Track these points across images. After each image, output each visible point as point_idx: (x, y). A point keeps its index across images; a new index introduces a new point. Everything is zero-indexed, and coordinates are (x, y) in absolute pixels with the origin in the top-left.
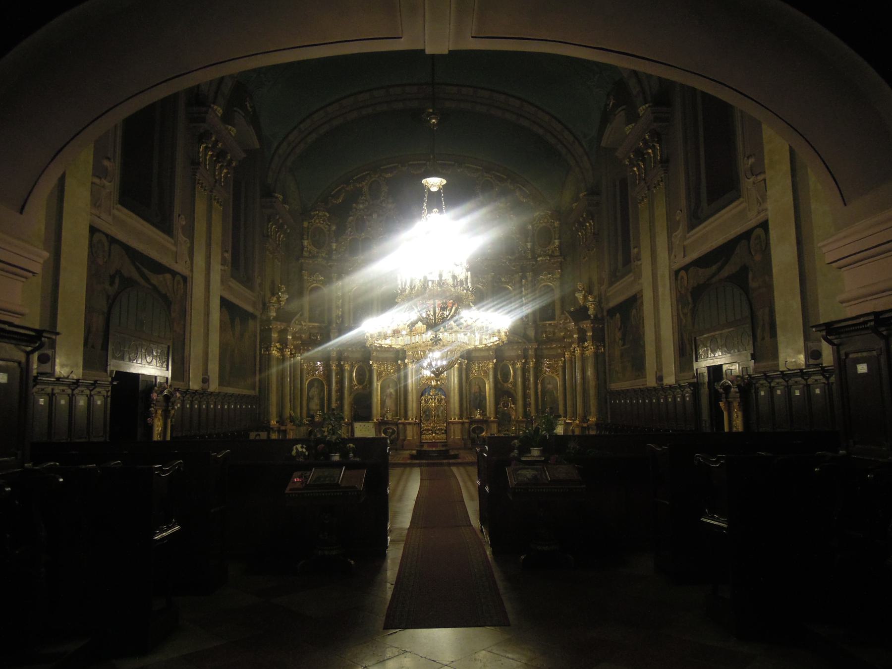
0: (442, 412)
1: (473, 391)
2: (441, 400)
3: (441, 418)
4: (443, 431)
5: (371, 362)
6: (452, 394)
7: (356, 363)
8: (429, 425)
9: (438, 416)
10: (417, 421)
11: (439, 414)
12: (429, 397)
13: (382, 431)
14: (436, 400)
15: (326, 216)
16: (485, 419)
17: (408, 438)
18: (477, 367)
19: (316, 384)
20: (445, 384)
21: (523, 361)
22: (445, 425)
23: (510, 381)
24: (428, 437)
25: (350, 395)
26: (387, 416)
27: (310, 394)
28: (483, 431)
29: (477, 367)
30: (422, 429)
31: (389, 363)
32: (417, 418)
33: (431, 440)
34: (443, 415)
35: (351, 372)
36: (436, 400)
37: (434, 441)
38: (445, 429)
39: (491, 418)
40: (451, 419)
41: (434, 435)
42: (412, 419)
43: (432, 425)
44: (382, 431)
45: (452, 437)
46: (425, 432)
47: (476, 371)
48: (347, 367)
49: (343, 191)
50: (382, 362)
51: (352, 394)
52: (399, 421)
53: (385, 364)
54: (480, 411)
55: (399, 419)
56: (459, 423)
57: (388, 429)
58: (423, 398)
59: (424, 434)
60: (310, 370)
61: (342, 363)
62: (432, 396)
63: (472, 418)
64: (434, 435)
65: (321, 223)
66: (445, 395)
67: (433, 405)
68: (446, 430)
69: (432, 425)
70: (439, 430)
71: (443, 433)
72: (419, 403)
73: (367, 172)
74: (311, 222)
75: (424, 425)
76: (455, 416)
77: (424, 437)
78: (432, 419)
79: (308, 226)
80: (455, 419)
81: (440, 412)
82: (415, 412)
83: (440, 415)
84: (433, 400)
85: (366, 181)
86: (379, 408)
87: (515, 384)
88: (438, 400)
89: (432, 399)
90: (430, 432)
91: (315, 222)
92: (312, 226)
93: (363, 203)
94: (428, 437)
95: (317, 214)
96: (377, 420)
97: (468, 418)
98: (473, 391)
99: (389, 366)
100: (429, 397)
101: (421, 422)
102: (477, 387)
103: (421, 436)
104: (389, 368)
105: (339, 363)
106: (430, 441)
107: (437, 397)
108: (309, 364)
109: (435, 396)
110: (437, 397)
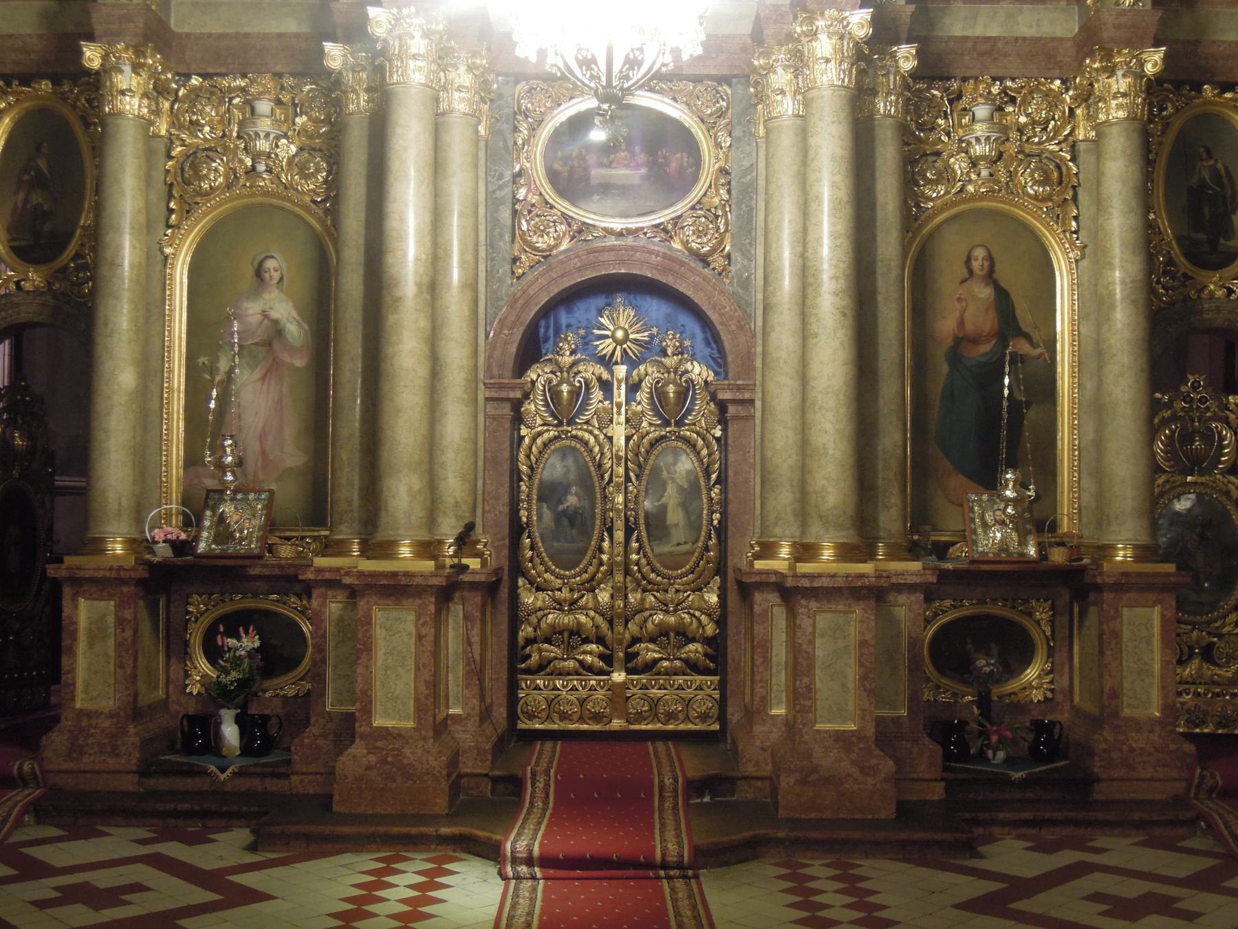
0: (691, 492)
1: (945, 326)
2: (682, 394)
3: (679, 534)
4: (694, 649)
5: (92, 56)
6: (783, 339)
8: (587, 599)
9: (657, 525)
10: (474, 563)
11: (663, 510)
12: (590, 370)
13: (195, 638)
14: (643, 395)
16: (1058, 556)
17: (379, 722)
18: (980, 129)
20: (718, 262)
22: (714, 599)
24: (568, 690)
26: (222, 519)
28: (1026, 662)
29: (980, 129)
30: (526, 631)
31: (267, 82)
32: (483, 538)
33: (597, 717)
34: (694, 526)
36: (643, 395)
37: (617, 724)
38: (710, 629)
39: (1105, 550)
40: (768, 550)
41: (619, 677)
42: (428, 548)
43: (604, 596)
44: (195, 638)
45: (779, 711)
46: (552, 651)
47: (974, 163)
50: (204, 76)
52: (320, 562)
54: (1022, 485)
55: (330, 547)
56: (856, 591)
57: (234, 623)
58: (538, 375)
59: (541, 668)
62: (607, 362)
63: (941, 550)
64: (619, 677)
66: (719, 361)
67: (619, 432)
68: (717, 646)
69: (604, 596)
70: (660, 635)
71: (692, 666)
72: (506, 410)
75: (542, 599)
76: (815, 532)
77: (535, 691)
78: (610, 550)
80: (805, 551)
81: (671, 496)
82: (454, 485)
83: (675, 516)
84: (620, 394)
86: (176, 452)
88: (658, 394)
89: (606, 386)
90: (590, 653)
94: (568, 690)
96: (139, 545)
97: (913, 551)
98: (945, 326)
99: (264, 107)
100: (590, 370)
101: (517, 569)
102: (985, 292)
103: (513, 686)
104: (265, 125)
106: (597, 727)
107: (650, 373)
109: (633, 364)
110: (650, 373)
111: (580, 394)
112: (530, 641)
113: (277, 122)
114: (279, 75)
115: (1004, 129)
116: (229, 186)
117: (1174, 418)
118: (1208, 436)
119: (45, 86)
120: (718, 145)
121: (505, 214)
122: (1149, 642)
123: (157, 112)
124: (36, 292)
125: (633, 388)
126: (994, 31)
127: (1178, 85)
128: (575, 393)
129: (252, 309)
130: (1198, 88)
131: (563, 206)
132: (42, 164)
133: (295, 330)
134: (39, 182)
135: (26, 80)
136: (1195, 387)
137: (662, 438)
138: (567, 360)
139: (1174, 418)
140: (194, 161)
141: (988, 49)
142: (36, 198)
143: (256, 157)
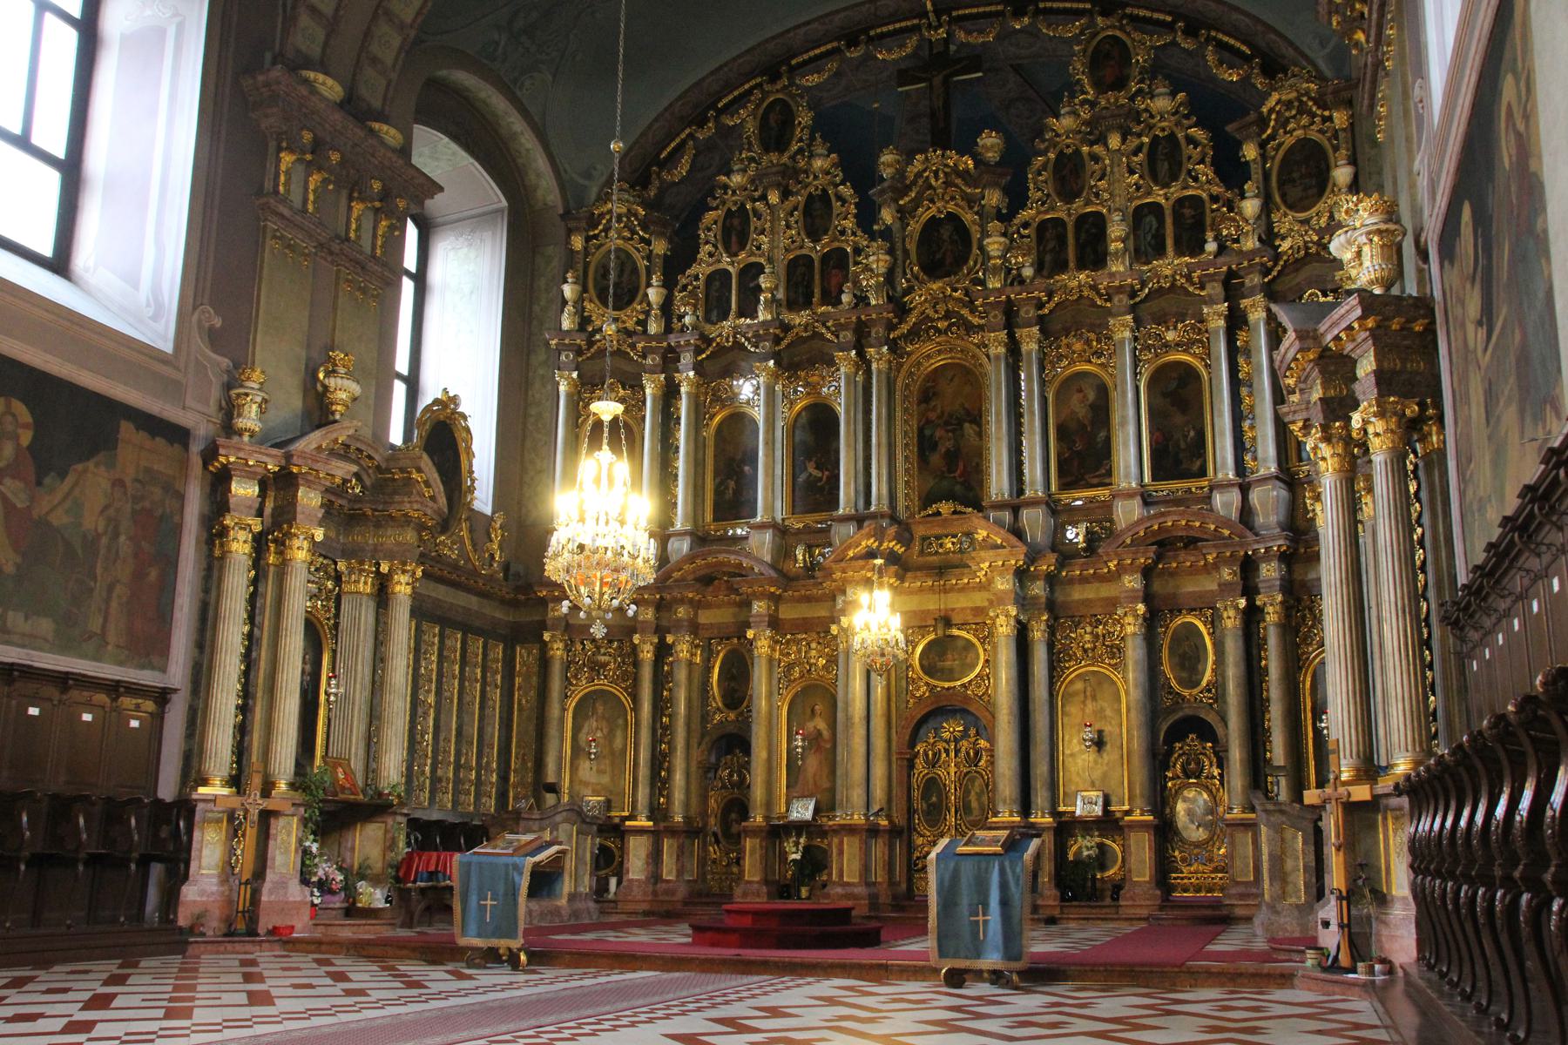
2: (976, 753)
7: (719, 644)
14: (962, 755)
15: (636, 215)
19: (600, 709)
21: (1242, 603)
23: (1204, 683)
25: (699, 744)
27: (582, 737)
29: (1088, 637)
35: (708, 670)
36: (962, 755)
47: (1085, 651)
48: (683, 650)
49: (691, 143)
51: (707, 739)
53: (798, 642)
58: (920, 748)
60: (584, 664)
61: (670, 639)
62: (948, 742)
65: (624, 238)
67: (953, 770)
72: (905, 763)
73: (753, 83)
74: (596, 237)
79: (586, 249)
83: (974, 804)
85: (751, 107)
87: (1218, 687)
89: (947, 751)
91: (606, 237)
92: (601, 245)
93: (744, 171)
95: (610, 212)
99: (813, 645)
100: (941, 745)
104: (813, 653)
105: (662, 640)
108: (579, 647)
109: (956, 741)
111: (937, 755)
112: (918, 858)
113: (819, 651)
114: (818, 633)
115: (1096, 636)
116: (801, 677)
117: (1184, 754)
118: (1198, 762)
119: (735, 640)
120: (985, 650)
121: (904, 683)
122: (1144, 848)
123: (773, 650)
124: (732, 721)
125: (957, 752)
126: (1091, 596)
127: (1171, 611)
128: (934, 755)
129: (810, 726)
130: (1180, 611)
131: (926, 678)
132: (734, 671)
133: (826, 734)
134: (733, 678)
135: (728, 639)
136: (1192, 740)
137: (968, 773)
138: (932, 741)
139: (1184, 754)
140: (790, 667)
141: (1087, 603)
142: (733, 684)
143: (811, 665)
